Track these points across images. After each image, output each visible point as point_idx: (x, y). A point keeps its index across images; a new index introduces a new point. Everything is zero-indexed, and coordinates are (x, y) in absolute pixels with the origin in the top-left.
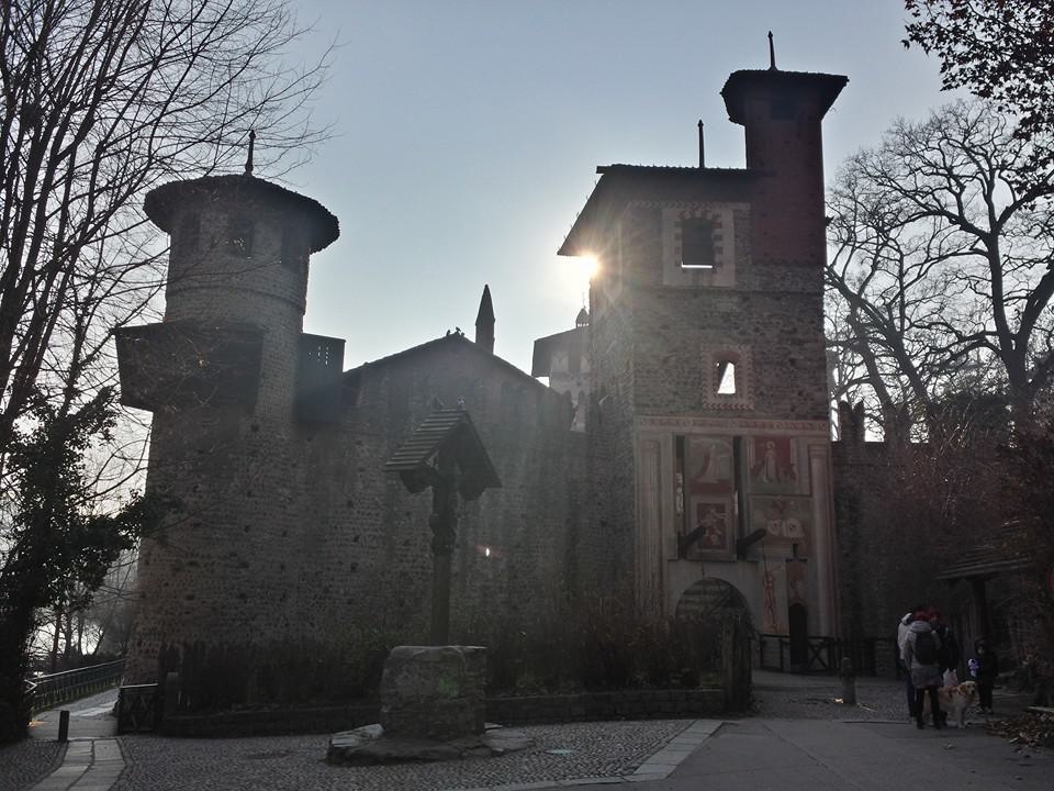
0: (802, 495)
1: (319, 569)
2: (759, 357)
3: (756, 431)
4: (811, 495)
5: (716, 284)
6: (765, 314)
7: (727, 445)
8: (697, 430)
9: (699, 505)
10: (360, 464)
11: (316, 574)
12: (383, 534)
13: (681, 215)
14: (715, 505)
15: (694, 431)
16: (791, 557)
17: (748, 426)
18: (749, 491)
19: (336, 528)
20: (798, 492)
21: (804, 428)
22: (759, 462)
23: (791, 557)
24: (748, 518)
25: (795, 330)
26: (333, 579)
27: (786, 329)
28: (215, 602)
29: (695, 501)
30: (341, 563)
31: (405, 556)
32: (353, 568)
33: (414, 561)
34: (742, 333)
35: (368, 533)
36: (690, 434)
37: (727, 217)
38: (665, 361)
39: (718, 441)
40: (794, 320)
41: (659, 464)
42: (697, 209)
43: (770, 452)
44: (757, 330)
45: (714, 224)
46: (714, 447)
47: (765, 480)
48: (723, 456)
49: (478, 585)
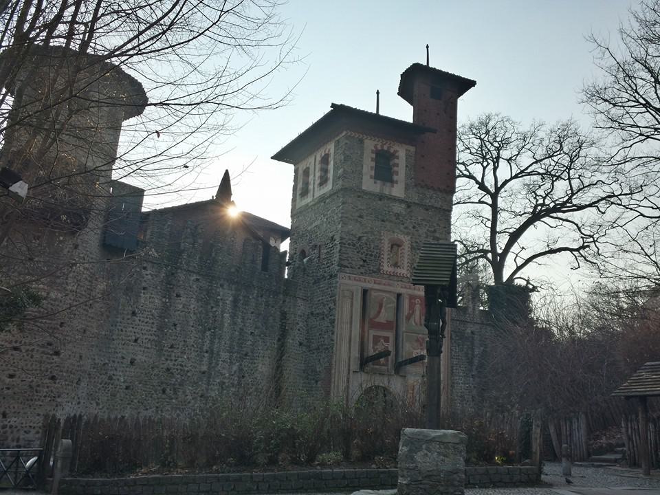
1: (107, 362)
2: (414, 244)
3: (410, 292)
5: (393, 194)
6: (420, 218)
8: (376, 287)
9: (374, 335)
10: (144, 284)
11: (104, 364)
12: (156, 339)
13: (376, 146)
14: (384, 337)
17: (405, 288)
18: (404, 329)
19: (122, 331)
22: (411, 312)
24: (402, 347)
25: (435, 231)
26: (116, 370)
27: (430, 229)
28: (32, 381)
29: (373, 333)
30: (123, 358)
31: (170, 356)
32: (132, 363)
33: (176, 360)
34: (406, 228)
35: (145, 337)
36: (372, 289)
37: (402, 153)
38: (360, 239)
39: (388, 295)
40: (435, 225)
41: (352, 306)
42: (385, 144)
44: (414, 227)
45: (393, 156)
47: (414, 324)
49: (218, 381)
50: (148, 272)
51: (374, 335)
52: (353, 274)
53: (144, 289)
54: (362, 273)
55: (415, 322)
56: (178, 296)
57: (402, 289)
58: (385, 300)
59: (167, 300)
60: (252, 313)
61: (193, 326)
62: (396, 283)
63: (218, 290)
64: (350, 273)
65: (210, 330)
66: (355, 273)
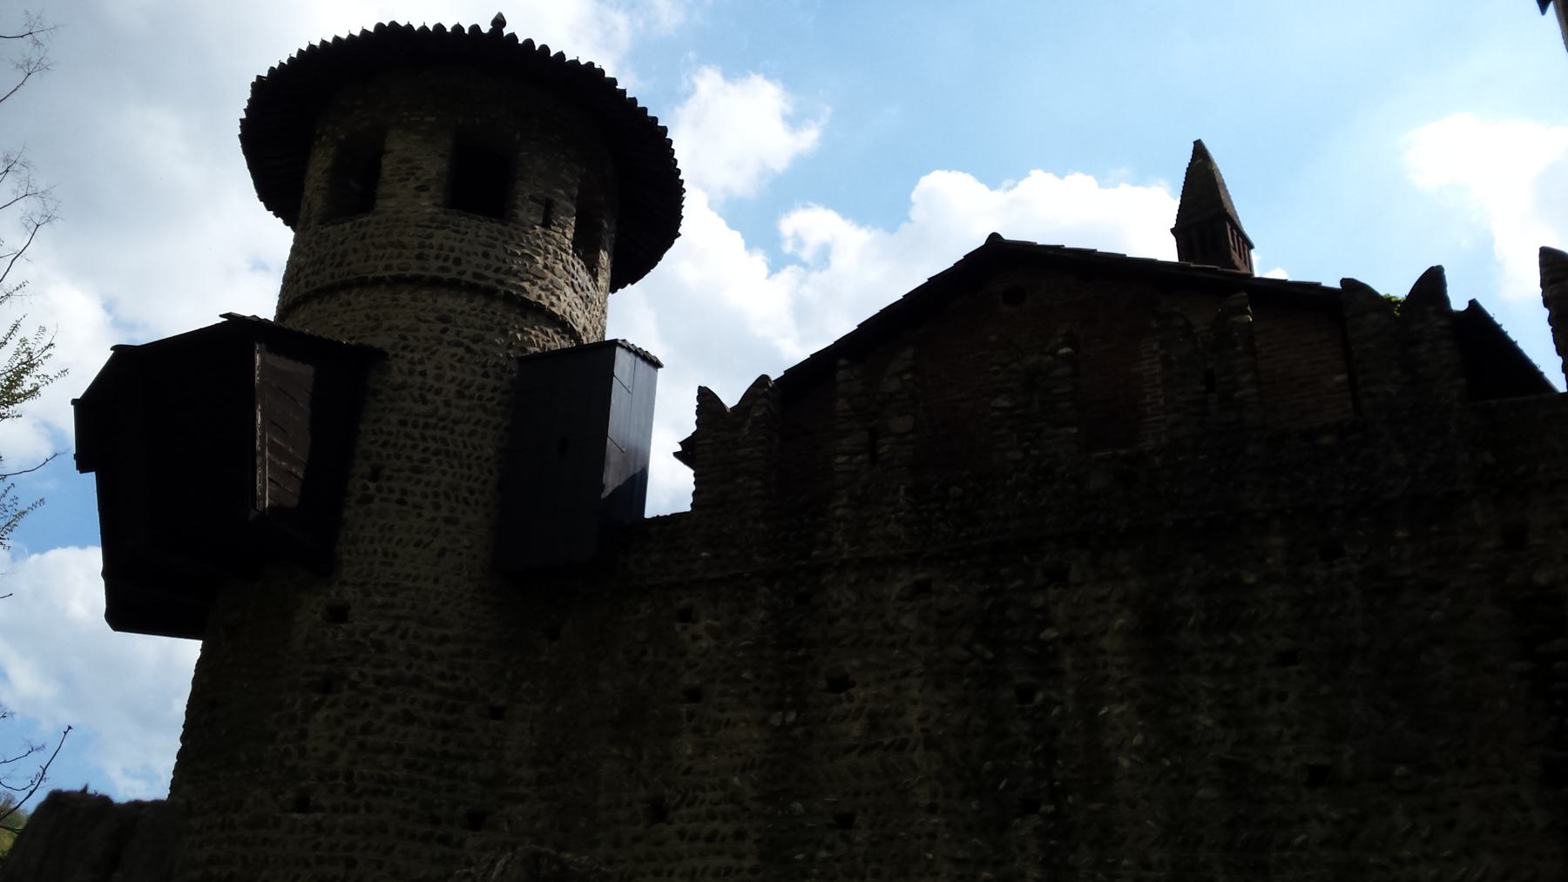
10: (689, 679)
50: (699, 628)
53: (694, 695)
56: (840, 684)
59: (791, 717)
60: (1287, 658)
61: (932, 809)
63: (1038, 601)
65: (1030, 807)
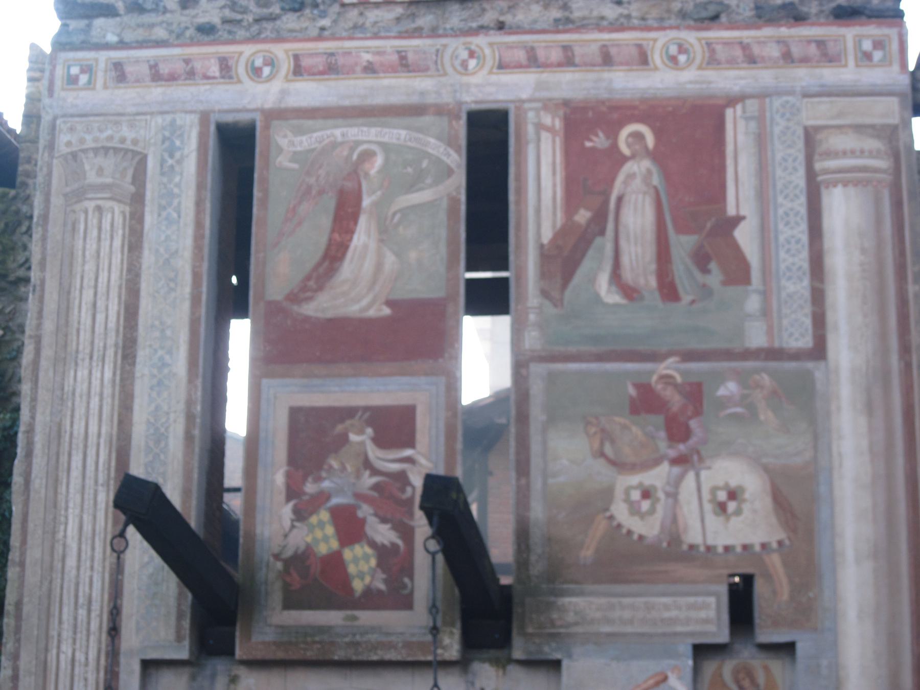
0: (774, 354)
4: (819, 351)
7: (436, 147)
9: (295, 413)
14: (366, 409)
15: (292, 102)
16: (722, 635)
17: (533, 61)
20: (756, 338)
21: (788, 57)
22: (583, 216)
23: (722, 635)
43: (630, 167)
46: (379, 161)
48: (416, 198)
51: (295, 413)
52: (142, 44)
54: (206, 30)
55: (616, 276)
57: (507, 78)
58: (379, 161)
62: (456, 47)
64: (122, 45)
66: (160, 33)
